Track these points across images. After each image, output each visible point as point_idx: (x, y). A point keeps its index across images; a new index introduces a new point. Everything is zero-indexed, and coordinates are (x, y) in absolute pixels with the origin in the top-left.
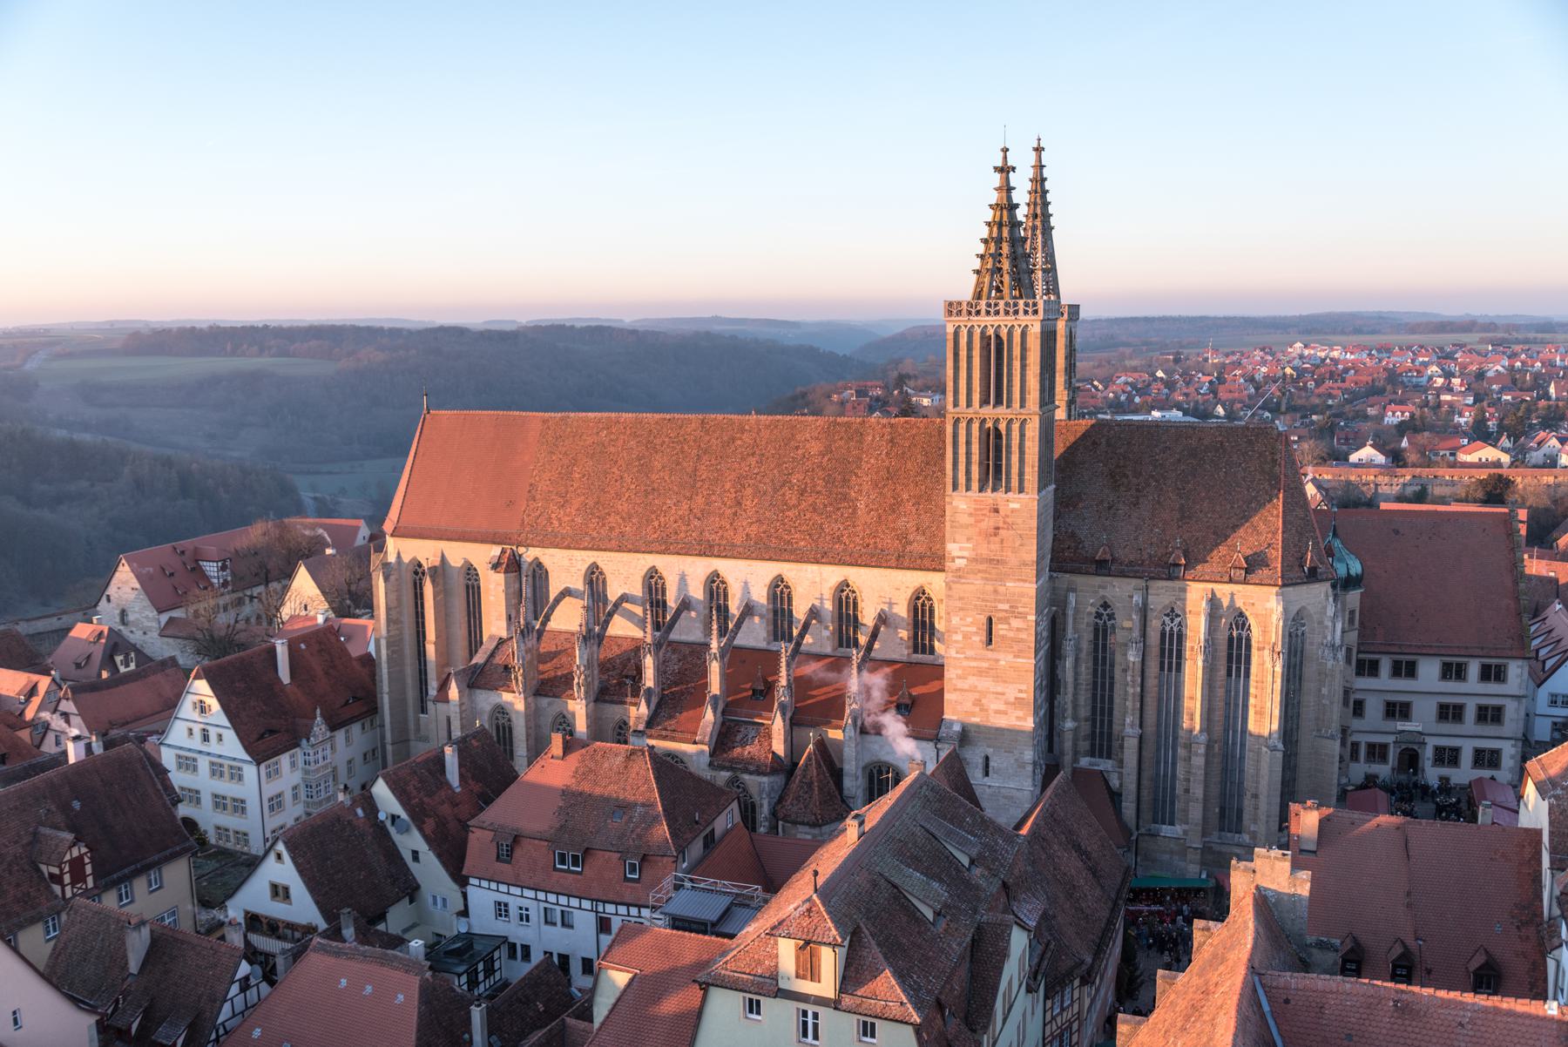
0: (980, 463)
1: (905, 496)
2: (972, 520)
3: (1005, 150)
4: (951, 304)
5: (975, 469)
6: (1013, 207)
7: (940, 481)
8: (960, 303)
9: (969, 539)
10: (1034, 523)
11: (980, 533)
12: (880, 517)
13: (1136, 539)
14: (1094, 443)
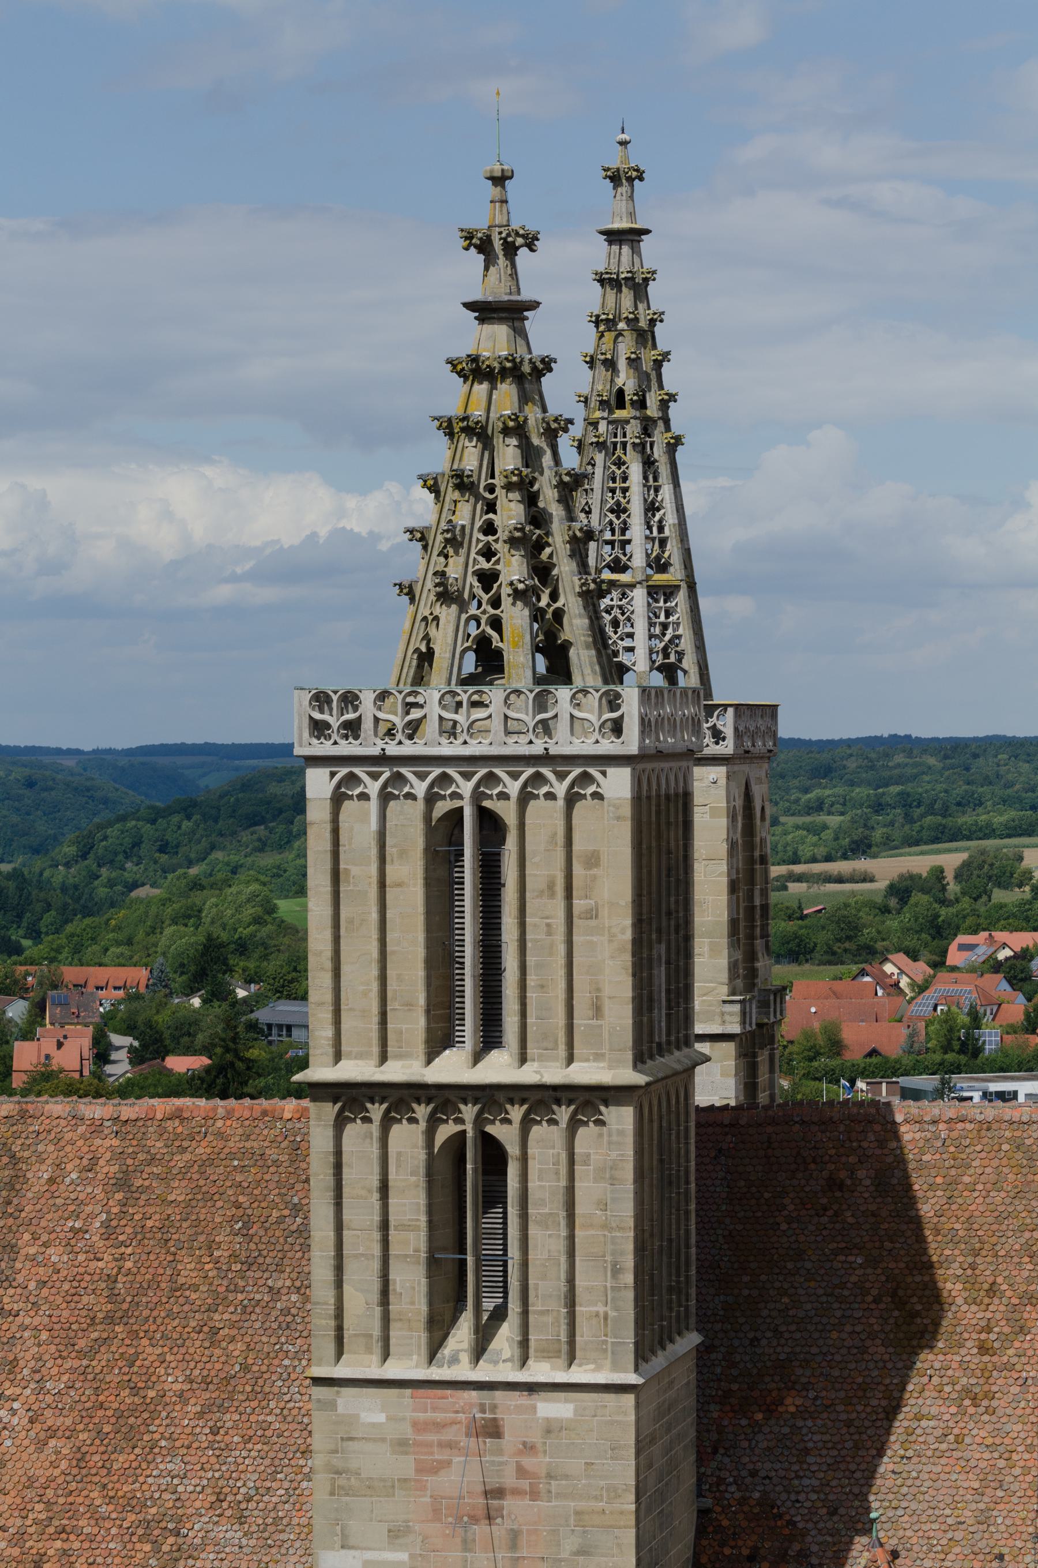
0: (433, 1263)
1: (173, 1382)
2: (406, 1466)
3: (500, 180)
4: (321, 699)
5: (411, 1284)
6: (527, 375)
7: (293, 1324)
8: (350, 699)
9: (396, 1535)
10: (624, 1472)
11: (436, 1513)
12: (80, 1459)
13: (984, 1520)
14: (834, 1184)
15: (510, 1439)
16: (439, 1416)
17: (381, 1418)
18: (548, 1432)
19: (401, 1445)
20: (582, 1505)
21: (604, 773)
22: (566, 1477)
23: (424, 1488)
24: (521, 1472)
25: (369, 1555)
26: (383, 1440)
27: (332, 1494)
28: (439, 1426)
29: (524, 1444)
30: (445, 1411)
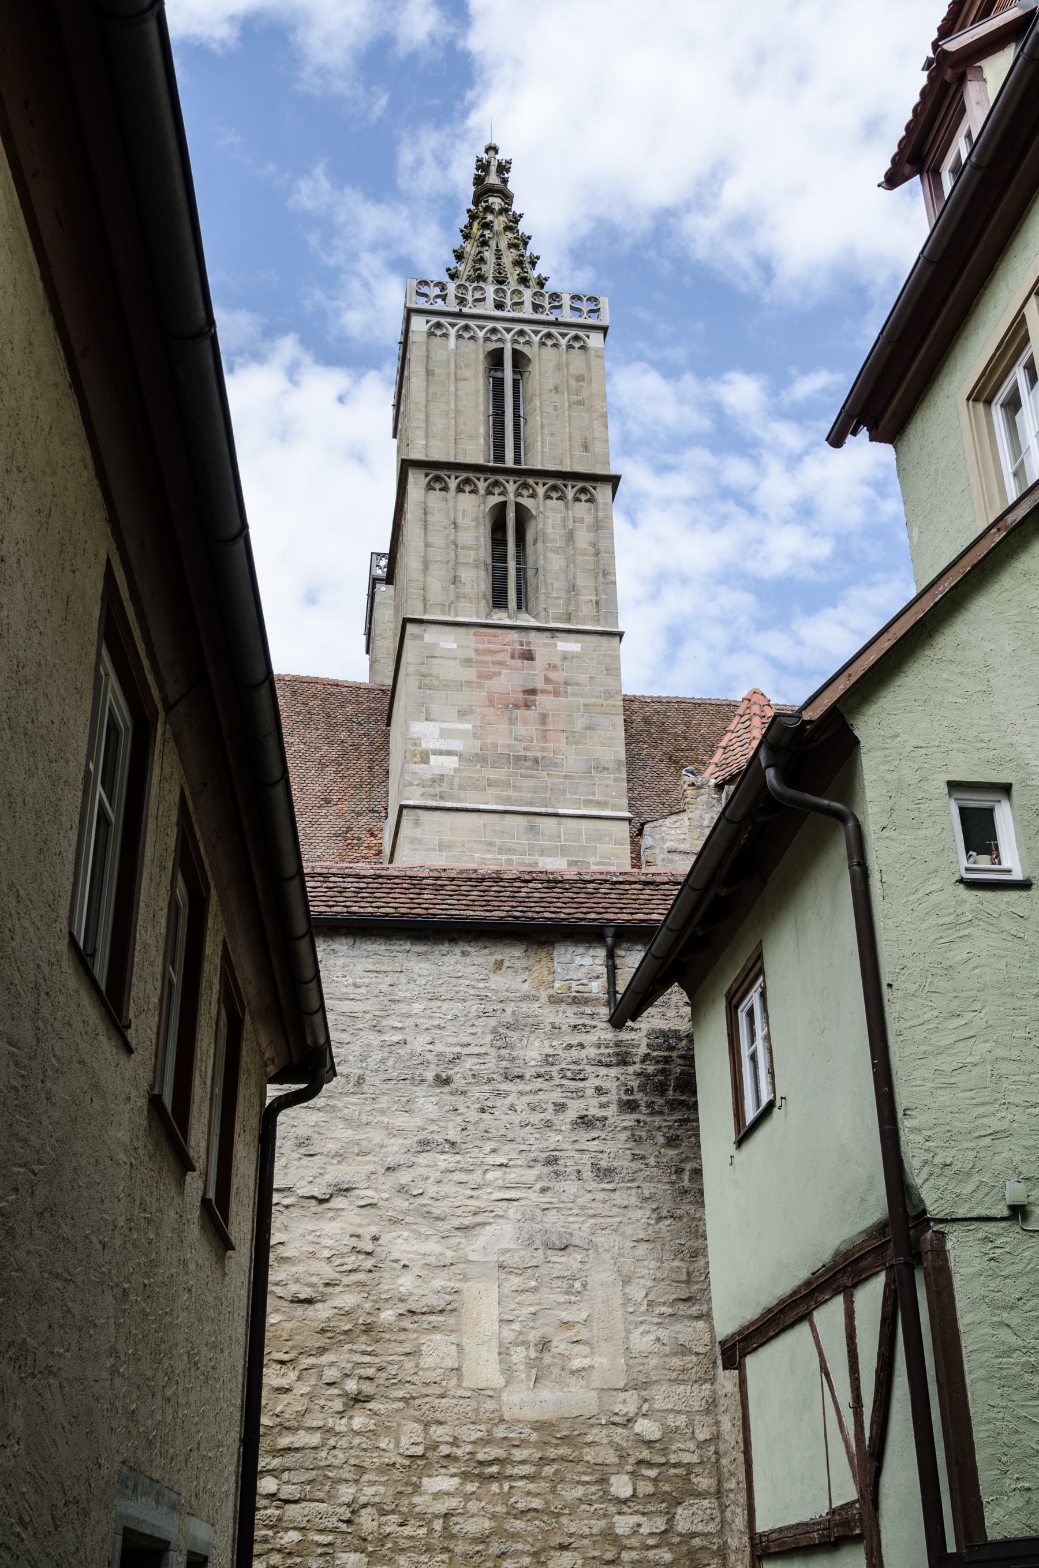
15: (540, 661)
16: (493, 647)
17: (454, 646)
18: (565, 658)
19: (468, 662)
20: (587, 701)
21: (588, 337)
22: (577, 684)
23: (482, 687)
24: (547, 680)
25: (444, 725)
26: (455, 658)
27: (420, 688)
28: (493, 652)
29: (549, 665)
30: (496, 643)
